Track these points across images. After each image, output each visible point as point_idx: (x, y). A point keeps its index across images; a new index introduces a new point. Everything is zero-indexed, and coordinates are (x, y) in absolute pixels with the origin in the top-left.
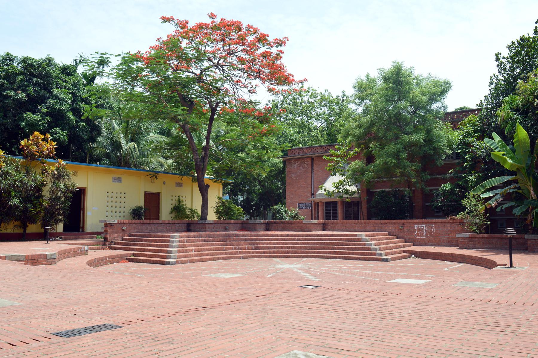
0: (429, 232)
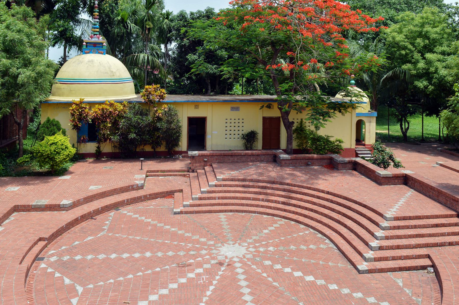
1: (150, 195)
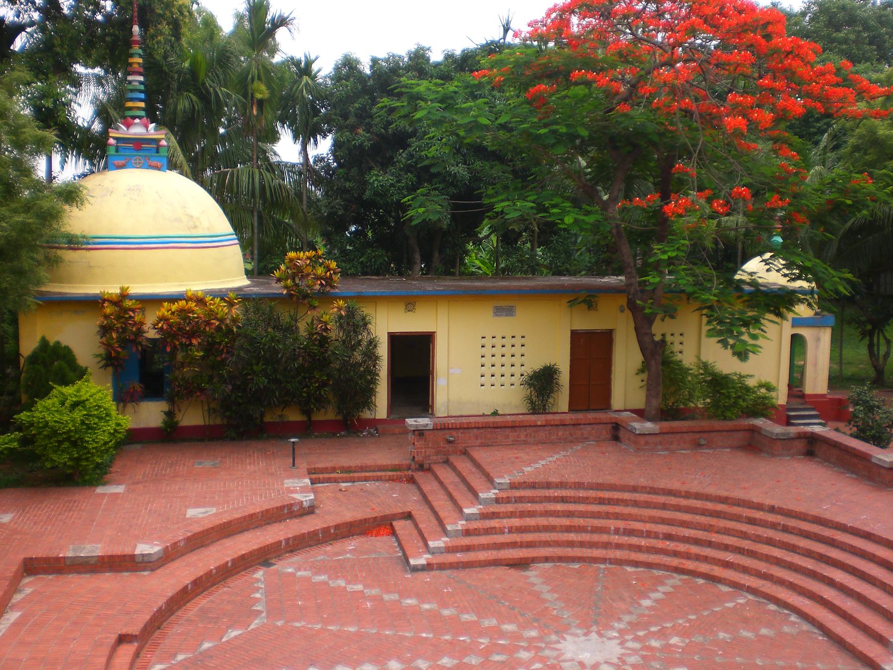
1: (337, 527)
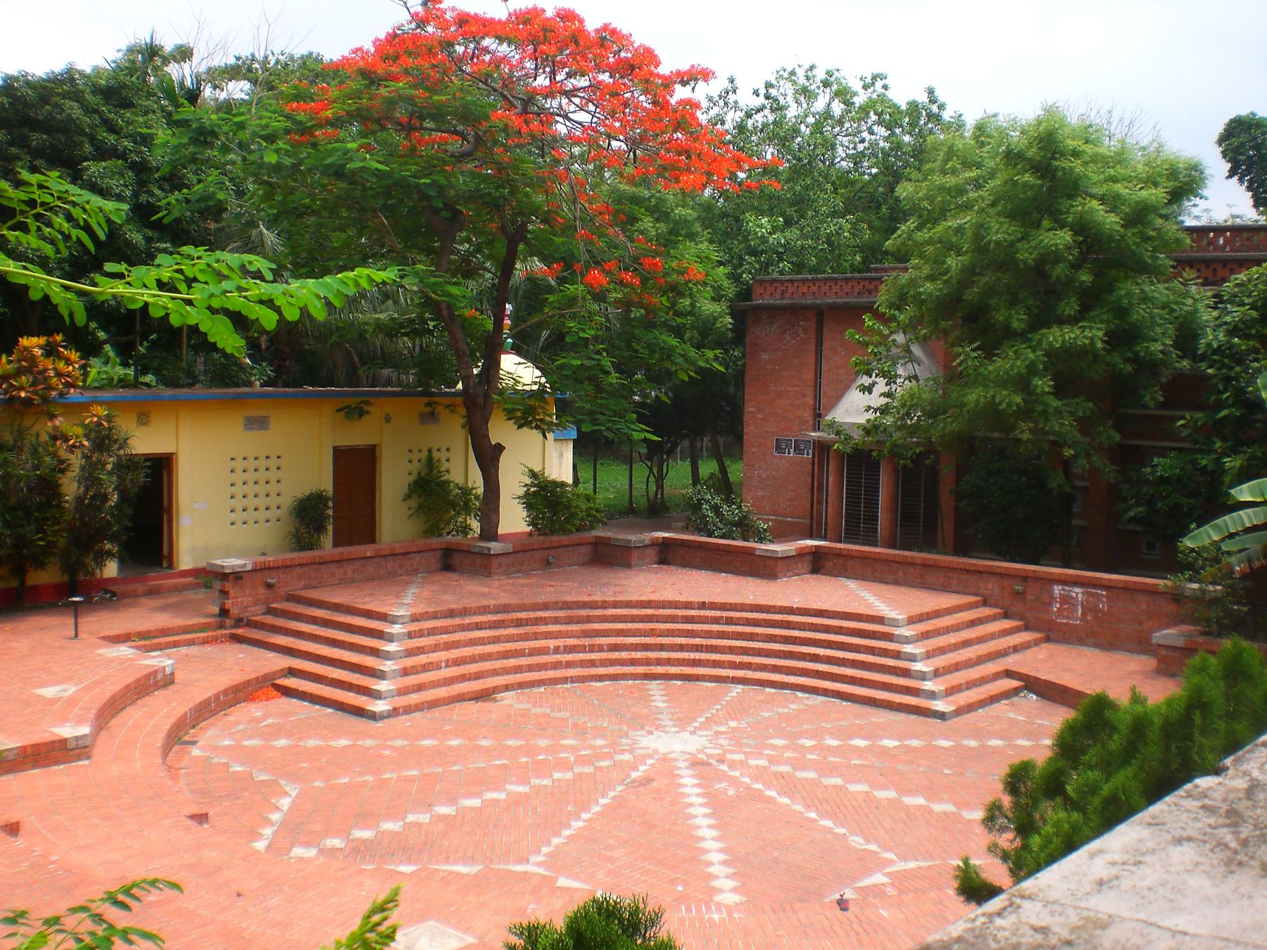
0: (1090, 610)
1: (226, 692)
